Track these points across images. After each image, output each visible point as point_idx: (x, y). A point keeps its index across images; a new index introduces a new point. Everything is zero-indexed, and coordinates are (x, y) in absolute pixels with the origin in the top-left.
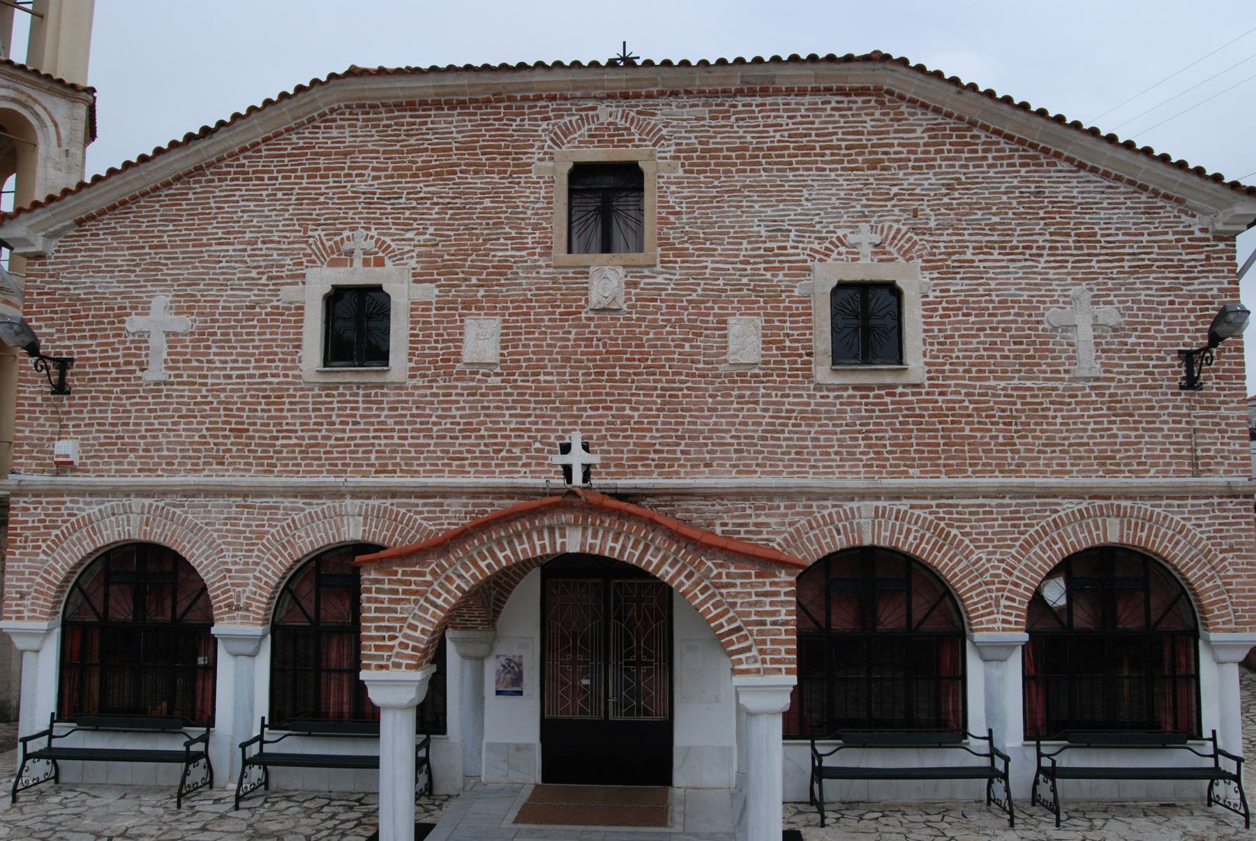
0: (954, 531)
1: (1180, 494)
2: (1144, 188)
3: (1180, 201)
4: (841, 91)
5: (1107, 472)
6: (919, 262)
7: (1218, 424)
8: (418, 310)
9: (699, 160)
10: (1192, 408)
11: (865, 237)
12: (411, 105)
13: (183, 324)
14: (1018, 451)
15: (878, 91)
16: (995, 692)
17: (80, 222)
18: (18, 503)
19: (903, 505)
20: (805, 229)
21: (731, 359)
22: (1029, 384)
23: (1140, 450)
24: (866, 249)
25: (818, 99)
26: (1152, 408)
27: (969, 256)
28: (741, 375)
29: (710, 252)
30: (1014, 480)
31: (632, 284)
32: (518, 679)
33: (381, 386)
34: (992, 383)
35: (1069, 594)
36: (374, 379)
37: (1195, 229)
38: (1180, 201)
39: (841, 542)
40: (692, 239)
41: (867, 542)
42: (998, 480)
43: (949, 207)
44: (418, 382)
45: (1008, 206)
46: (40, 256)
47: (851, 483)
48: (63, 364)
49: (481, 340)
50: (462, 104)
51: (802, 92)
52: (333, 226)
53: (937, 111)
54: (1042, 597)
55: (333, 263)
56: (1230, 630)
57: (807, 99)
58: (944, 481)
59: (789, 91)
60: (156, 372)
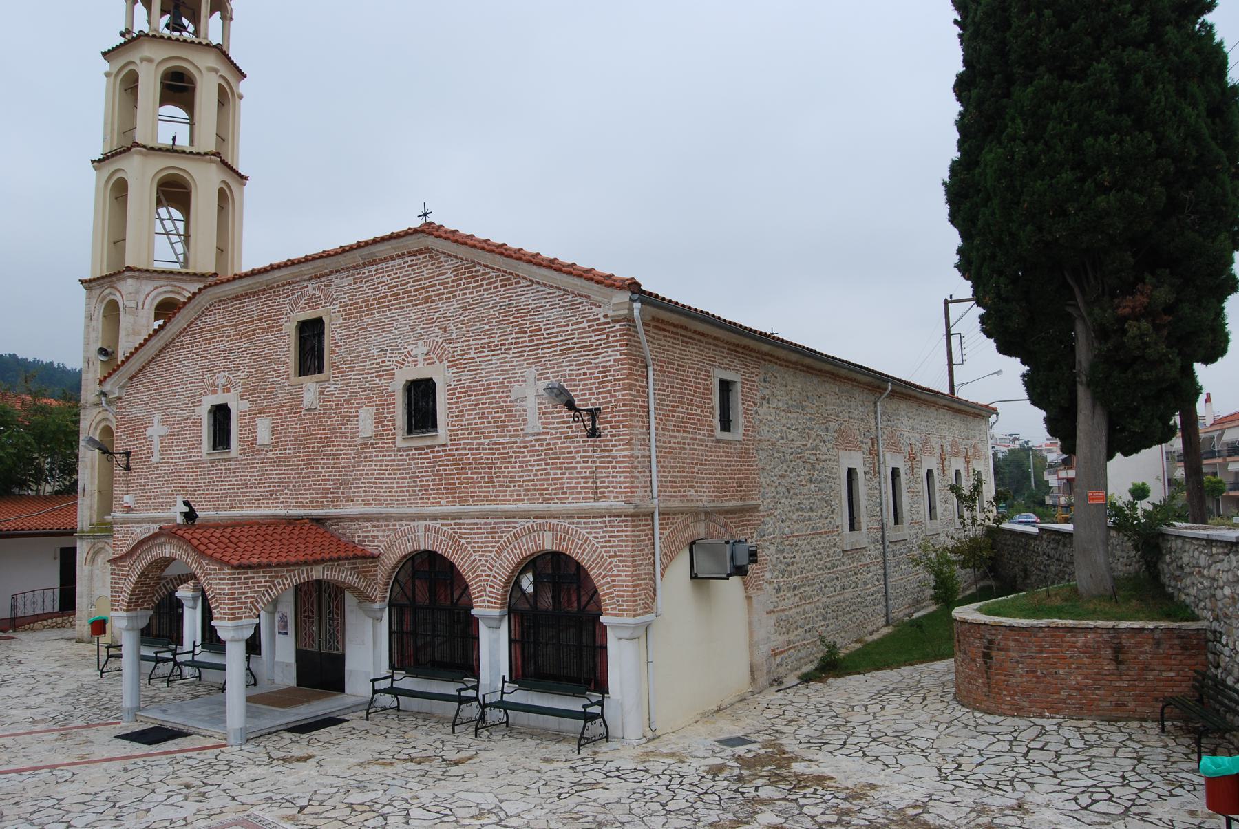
0: (463, 541)
1: (584, 515)
2: (567, 292)
3: (587, 297)
4: (410, 254)
5: (544, 499)
6: (446, 362)
7: (610, 462)
8: (242, 414)
9: (350, 310)
10: (594, 451)
11: (420, 350)
12: (237, 298)
13: (164, 430)
14: (494, 487)
15: (427, 250)
16: (494, 649)
17: (131, 379)
18: (116, 527)
19: (438, 524)
20: (394, 348)
21: (361, 434)
22: (501, 440)
23: (562, 483)
24: (420, 358)
25: (402, 261)
26: (570, 452)
27: (472, 355)
28: (365, 446)
29: (352, 369)
30: (493, 507)
31: (322, 393)
32: (285, 626)
33: (230, 460)
34: (482, 441)
35: (535, 583)
36: (226, 456)
37: (600, 316)
38: (587, 297)
39: (410, 548)
40: (346, 362)
41: (422, 548)
42: (487, 507)
43: (463, 323)
44: (241, 457)
45: (493, 317)
46: (120, 398)
47: (413, 510)
48: (128, 454)
49: (264, 434)
50: (255, 294)
51: (392, 258)
52: (213, 371)
53: (455, 257)
54: (521, 588)
55: (214, 392)
56: (616, 615)
57: (397, 261)
58: (457, 508)
59: (386, 259)
60: (156, 459)
